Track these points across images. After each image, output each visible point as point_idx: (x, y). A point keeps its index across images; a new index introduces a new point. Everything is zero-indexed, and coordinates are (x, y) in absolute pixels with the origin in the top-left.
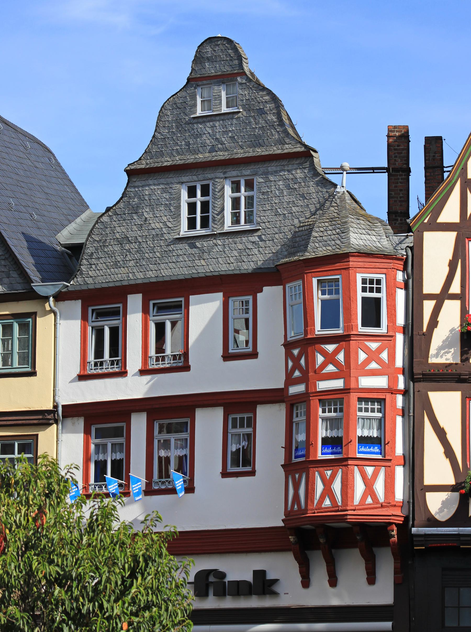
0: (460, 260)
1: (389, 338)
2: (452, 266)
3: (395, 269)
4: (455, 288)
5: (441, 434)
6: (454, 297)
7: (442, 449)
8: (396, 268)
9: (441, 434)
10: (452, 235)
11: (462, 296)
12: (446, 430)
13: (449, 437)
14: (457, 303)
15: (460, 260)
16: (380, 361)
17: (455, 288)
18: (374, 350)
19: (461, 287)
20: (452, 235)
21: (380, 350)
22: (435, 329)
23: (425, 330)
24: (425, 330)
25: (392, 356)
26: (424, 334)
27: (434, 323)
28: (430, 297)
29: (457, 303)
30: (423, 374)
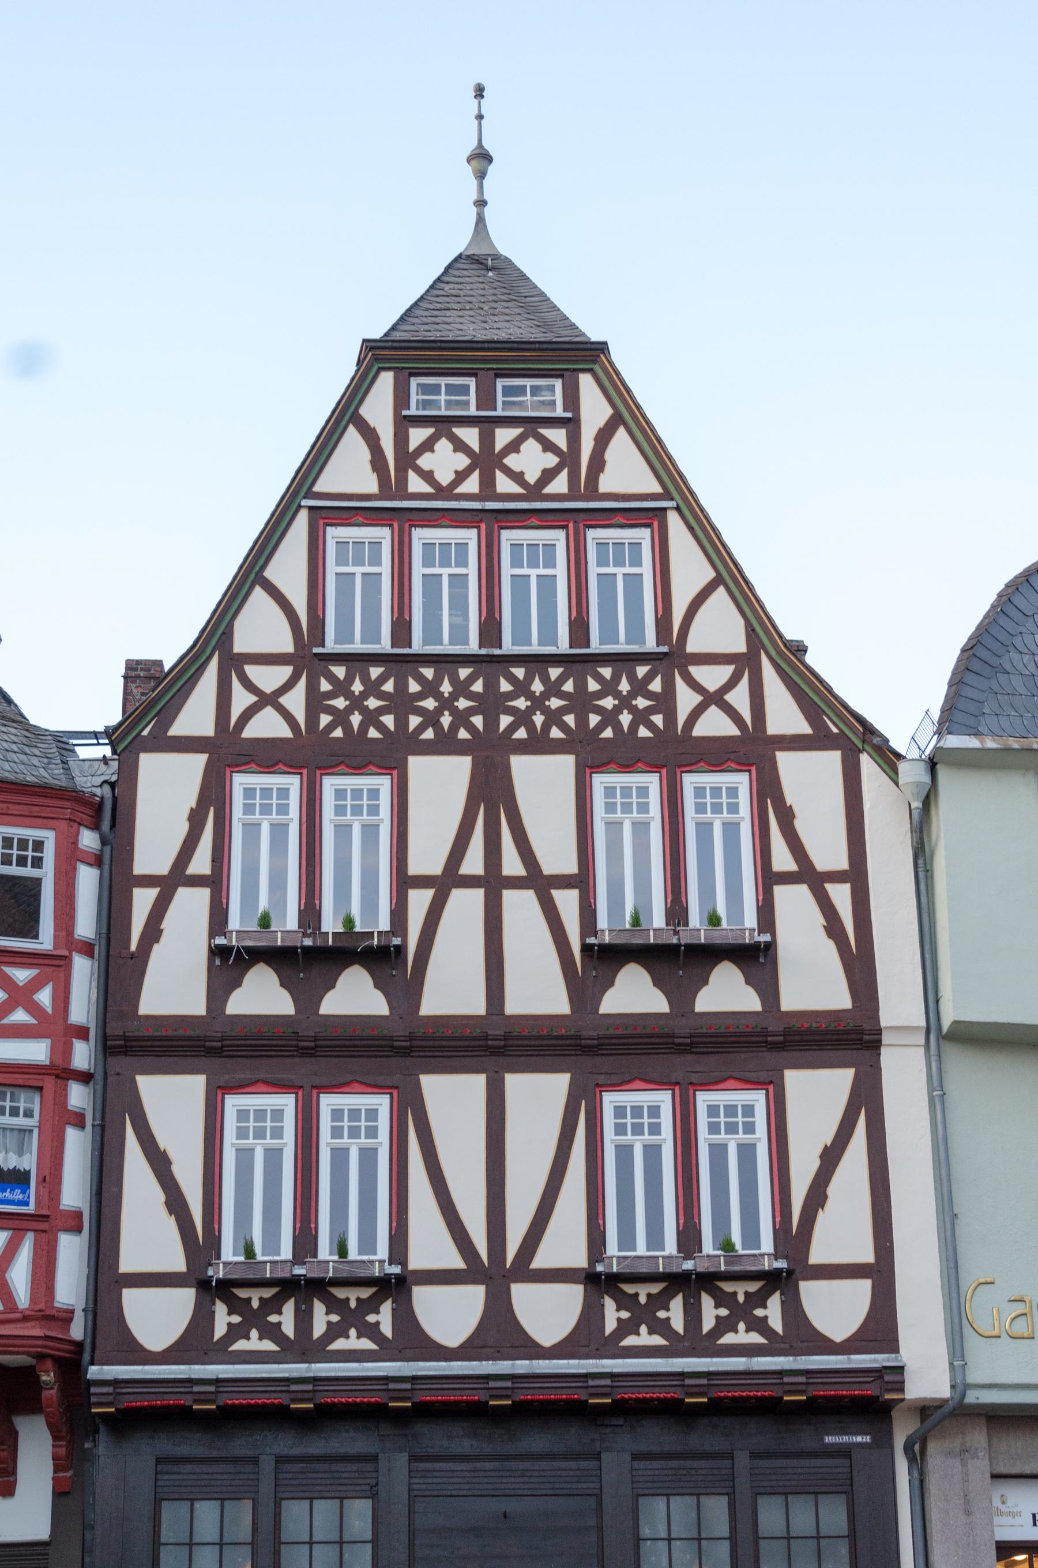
0: (212, 808)
1: (54, 966)
2: (196, 819)
3: (75, 821)
4: (201, 863)
5: (160, 1163)
6: (197, 881)
7: (161, 1197)
8: (78, 820)
9: (160, 1163)
10: (200, 760)
11: (216, 882)
12: (172, 1155)
13: (177, 1170)
14: (203, 894)
15: (212, 808)
16: (34, 1008)
17: (201, 863)
18: (21, 984)
19: (213, 861)
20: (202, 759)
21: (35, 985)
22: (156, 946)
23: (133, 947)
24: (133, 947)
25: (62, 999)
26: (132, 956)
27: (153, 932)
28: (148, 881)
29: (203, 894)
30: (126, 1039)
